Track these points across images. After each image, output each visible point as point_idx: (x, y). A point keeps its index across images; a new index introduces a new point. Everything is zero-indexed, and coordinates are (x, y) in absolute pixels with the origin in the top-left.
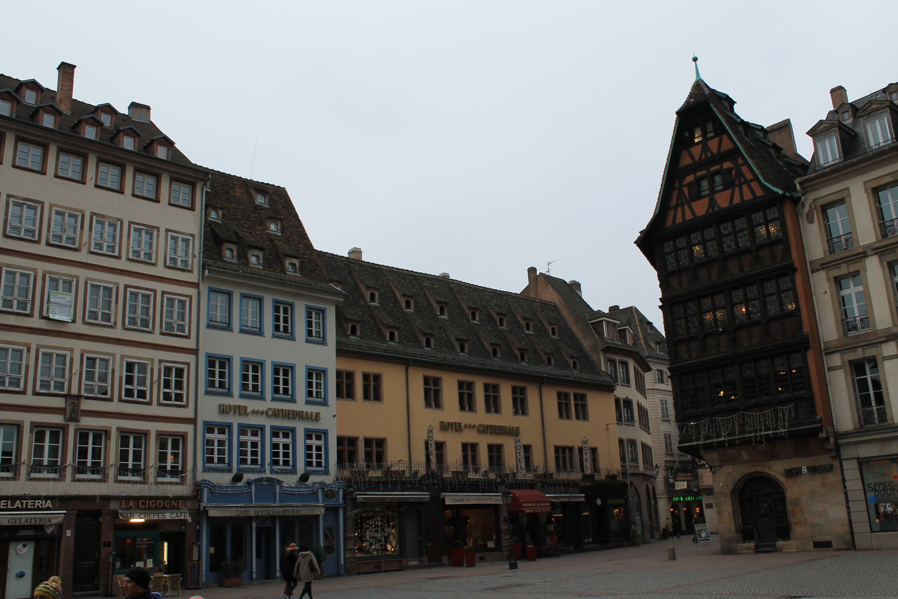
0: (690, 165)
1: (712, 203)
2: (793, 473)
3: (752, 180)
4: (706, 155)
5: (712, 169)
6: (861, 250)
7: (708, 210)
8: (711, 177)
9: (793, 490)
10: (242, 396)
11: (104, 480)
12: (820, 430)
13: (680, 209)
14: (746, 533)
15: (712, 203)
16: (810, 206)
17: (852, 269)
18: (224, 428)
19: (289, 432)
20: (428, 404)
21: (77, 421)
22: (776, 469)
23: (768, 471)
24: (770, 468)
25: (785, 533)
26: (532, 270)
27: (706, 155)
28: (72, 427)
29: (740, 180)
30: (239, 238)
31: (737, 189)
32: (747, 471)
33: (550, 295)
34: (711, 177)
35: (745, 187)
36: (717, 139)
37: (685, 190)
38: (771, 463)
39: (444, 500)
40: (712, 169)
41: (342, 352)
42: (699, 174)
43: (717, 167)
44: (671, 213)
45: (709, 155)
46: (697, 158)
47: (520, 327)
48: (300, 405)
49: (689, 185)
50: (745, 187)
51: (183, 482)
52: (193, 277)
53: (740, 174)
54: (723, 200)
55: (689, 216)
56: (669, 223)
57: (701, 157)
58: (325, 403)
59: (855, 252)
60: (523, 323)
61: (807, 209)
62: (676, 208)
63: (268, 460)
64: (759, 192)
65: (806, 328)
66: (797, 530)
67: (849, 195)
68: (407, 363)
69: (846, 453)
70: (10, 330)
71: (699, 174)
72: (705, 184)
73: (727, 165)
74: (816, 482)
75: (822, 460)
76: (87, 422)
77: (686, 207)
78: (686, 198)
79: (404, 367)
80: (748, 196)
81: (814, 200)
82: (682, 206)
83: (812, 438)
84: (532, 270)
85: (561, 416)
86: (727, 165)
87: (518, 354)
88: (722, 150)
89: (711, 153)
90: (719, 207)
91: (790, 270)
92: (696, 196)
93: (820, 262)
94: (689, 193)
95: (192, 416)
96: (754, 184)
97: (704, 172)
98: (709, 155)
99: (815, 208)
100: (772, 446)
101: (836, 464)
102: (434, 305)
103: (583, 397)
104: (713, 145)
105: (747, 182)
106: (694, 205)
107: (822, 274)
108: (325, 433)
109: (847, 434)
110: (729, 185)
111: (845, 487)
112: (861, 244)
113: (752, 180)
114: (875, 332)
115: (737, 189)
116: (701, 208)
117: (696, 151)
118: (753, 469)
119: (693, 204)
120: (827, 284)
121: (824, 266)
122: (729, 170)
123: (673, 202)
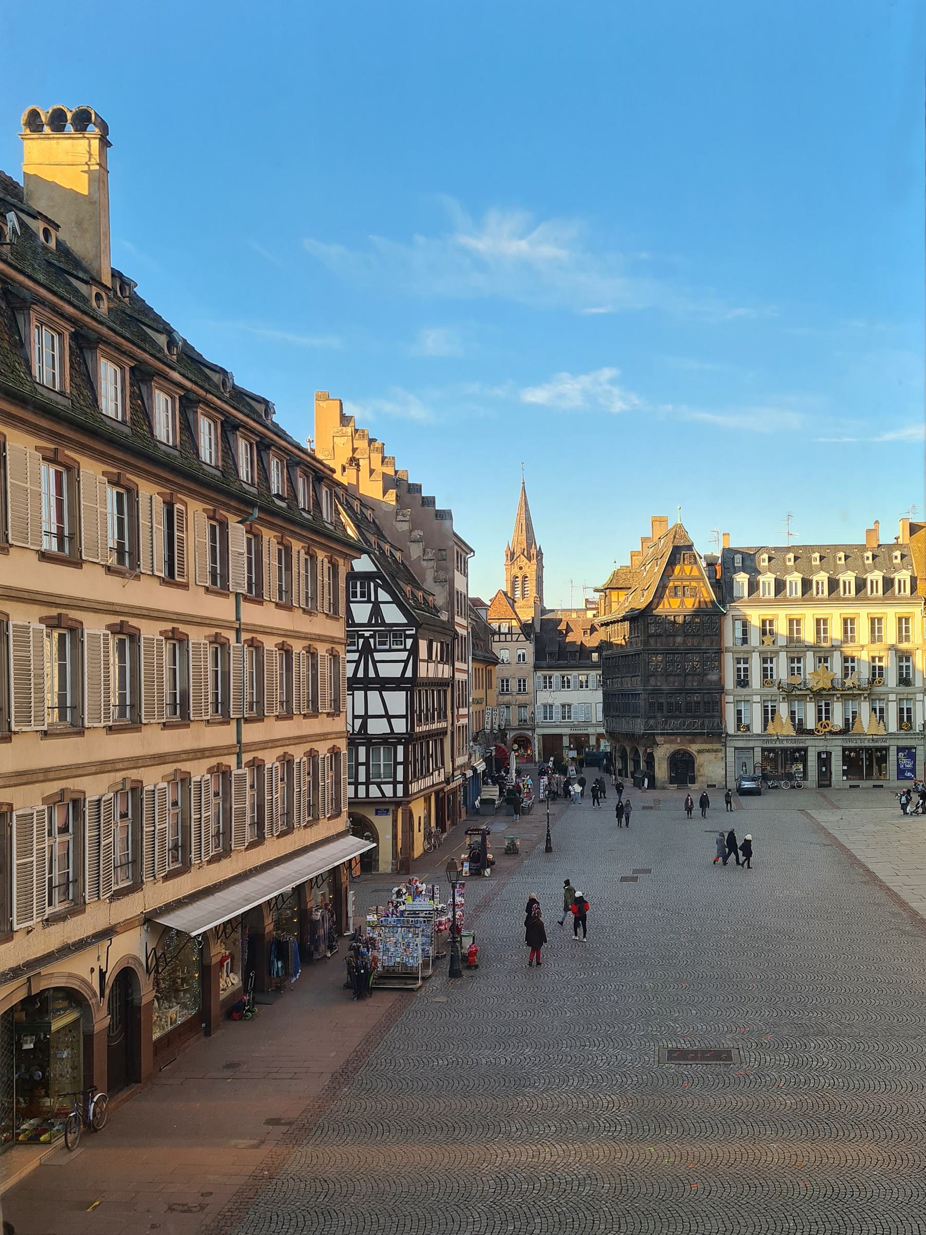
2: (699, 752)
9: (700, 759)
12: (722, 733)
14: (672, 780)
15: (682, 603)
22: (693, 748)
25: (693, 781)
66: (700, 779)
69: (728, 744)
73: (694, 584)
74: (712, 756)
75: (717, 746)
83: (717, 735)
86: (694, 584)
91: (720, 652)
100: (694, 737)
101: (723, 748)
109: (730, 736)
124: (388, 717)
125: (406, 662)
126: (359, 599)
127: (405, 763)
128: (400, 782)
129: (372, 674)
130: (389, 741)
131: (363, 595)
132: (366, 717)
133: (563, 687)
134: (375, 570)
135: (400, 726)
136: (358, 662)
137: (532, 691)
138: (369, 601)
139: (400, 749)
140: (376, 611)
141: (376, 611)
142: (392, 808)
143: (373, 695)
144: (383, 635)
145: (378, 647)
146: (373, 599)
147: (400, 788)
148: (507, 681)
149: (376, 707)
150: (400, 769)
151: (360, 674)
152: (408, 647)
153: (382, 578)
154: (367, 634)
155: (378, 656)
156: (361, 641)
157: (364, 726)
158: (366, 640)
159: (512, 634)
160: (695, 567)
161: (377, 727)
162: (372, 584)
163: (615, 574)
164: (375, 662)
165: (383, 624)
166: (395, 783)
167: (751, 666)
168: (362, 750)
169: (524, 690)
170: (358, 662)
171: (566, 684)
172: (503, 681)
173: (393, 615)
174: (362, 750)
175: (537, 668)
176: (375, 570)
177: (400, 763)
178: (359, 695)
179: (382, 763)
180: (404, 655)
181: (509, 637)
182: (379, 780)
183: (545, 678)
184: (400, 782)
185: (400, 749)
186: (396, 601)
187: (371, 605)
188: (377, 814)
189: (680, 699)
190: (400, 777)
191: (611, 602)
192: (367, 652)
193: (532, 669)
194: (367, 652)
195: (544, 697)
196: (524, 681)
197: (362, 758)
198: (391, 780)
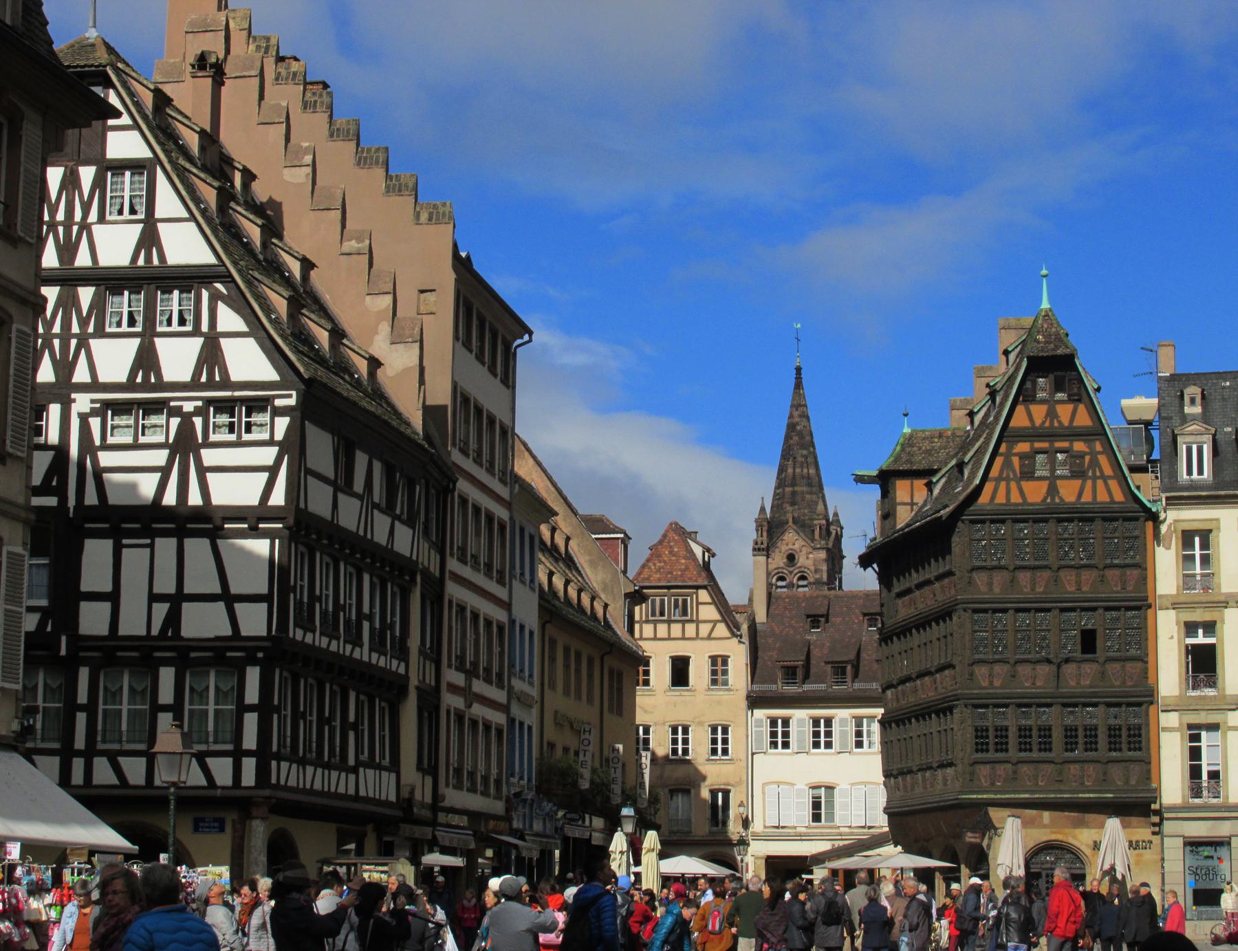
0: (1027, 428)
1: (1053, 490)
3: (1110, 477)
4: (1052, 422)
5: (1058, 445)
6: (1223, 598)
7: (1045, 499)
8: (1051, 453)
13: (1003, 484)
15: (1053, 490)
16: (1169, 527)
17: (1206, 616)
21: (470, 706)
23: (1071, 841)
24: (1075, 837)
27: (1052, 422)
29: (1094, 472)
31: (1089, 483)
32: (1045, 838)
34: (1051, 453)
35: (1100, 483)
36: (1070, 407)
37: (1015, 460)
38: (1077, 831)
40: (1058, 445)
42: (1038, 445)
43: (1065, 444)
44: (988, 488)
45: (1056, 424)
46: (1038, 422)
49: (1022, 456)
50: (1100, 483)
51: (498, 797)
52: (504, 492)
53: (1095, 463)
54: (1068, 492)
55: (1015, 498)
56: (984, 498)
57: (1044, 422)
59: (1216, 599)
61: (1164, 529)
62: (999, 479)
64: (1119, 496)
65: (1150, 681)
67: (1219, 528)
69: (1168, 827)
71: (1038, 445)
72: (1040, 458)
73: (1079, 446)
76: (478, 710)
77: (1013, 485)
78: (1014, 472)
80: (1102, 497)
81: (1175, 521)
82: (1008, 480)
83: (1139, 807)
88: (1075, 424)
89: (1060, 422)
90: (1061, 498)
91: (1139, 605)
92: (1028, 474)
93: (1172, 600)
94: (1021, 466)
96: (1113, 484)
97: (1045, 445)
98: (1056, 424)
99: (1175, 531)
101: (1156, 839)
103: (620, 675)
104: (1064, 412)
105: (1104, 478)
106: (1026, 485)
107: (1172, 613)
109: (1173, 808)
110: (1078, 473)
111: (1163, 867)
112: (1224, 590)
113: (1110, 477)
114: (1225, 696)
115: (1089, 483)
116: (1035, 492)
117: (1039, 412)
118: (1053, 837)
119: (1024, 484)
120: (1176, 628)
121: (1175, 606)
122: (1081, 456)
123: (994, 472)
124: (228, 598)
125: (273, 471)
126: (175, 327)
127: (265, 709)
128: (249, 753)
129: (195, 499)
130: (226, 654)
131: (182, 322)
132: (177, 599)
133: (816, 745)
134: (212, 260)
135: (254, 620)
136: (165, 471)
137: (743, 757)
138: (196, 332)
139: (253, 675)
140: (211, 355)
141: (211, 355)
142: (230, 817)
143: (197, 548)
144: (224, 406)
145: (213, 438)
146: (205, 327)
147: (249, 764)
148: (686, 731)
149: (201, 578)
150: (251, 721)
151: (170, 499)
152: (279, 435)
153: (227, 278)
155: (210, 457)
156: (175, 422)
157: (173, 619)
158: (187, 419)
159: (698, 622)
160: (1081, 407)
161: (202, 622)
162: (205, 295)
163: (910, 441)
164: (202, 471)
165: (226, 383)
166: (238, 755)
167: (1221, 641)
168: (167, 676)
169: (725, 752)
170: (165, 471)
171: (821, 737)
172: (675, 731)
173: (248, 362)
174: (167, 676)
175: (755, 701)
176: (212, 260)
177: (251, 708)
178: (166, 547)
179: (211, 707)
181: (690, 629)
182: (203, 747)
183: (773, 722)
184: (249, 753)
185: (253, 675)
186: (256, 330)
187: (198, 342)
188: (196, 829)
189: (1052, 717)
190: (250, 740)
191: (894, 505)
192: (185, 446)
193: (744, 704)
194: (185, 446)
195: (772, 766)
196: (725, 730)
197: (166, 695)
198: (229, 747)
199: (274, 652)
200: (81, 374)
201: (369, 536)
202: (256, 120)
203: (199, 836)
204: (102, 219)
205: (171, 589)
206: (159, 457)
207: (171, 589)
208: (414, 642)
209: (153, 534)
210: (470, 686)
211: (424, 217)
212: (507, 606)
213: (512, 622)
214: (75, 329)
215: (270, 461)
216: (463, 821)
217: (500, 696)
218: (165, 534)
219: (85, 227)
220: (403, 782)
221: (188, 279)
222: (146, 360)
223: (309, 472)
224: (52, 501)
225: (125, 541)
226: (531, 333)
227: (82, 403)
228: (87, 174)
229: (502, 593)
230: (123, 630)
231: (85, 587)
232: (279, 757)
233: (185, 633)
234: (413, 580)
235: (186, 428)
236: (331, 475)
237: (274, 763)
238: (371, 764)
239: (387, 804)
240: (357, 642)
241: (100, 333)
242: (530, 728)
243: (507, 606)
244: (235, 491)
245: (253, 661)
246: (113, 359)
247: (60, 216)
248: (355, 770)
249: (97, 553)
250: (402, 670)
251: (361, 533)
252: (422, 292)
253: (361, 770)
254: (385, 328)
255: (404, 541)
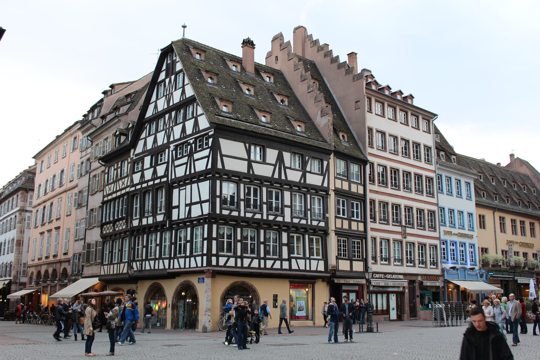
10: (450, 227)
11: (414, 266)
18: (444, 242)
19: (463, 245)
20: (501, 232)
21: (405, 238)
26: (512, 156)
28: (404, 241)
30: (442, 148)
33: (523, 170)
39: (517, 280)
41: (478, 205)
47: (521, 189)
48: (466, 232)
51: (437, 268)
52: (432, 168)
58: (473, 231)
60: (522, 187)
63: (459, 259)
68: (494, 209)
70: (383, 195)
76: (410, 239)
79: (491, 212)
84: (512, 156)
85: (531, 236)
87: (527, 204)
95: (438, 236)
102: (489, 177)
108: (474, 245)
125: (208, 157)
127: (210, 239)
129: (193, 171)
140: (196, 124)
141: (196, 124)
147: (205, 258)
151: (188, 173)
152: (210, 145)
154: (191, 141)
155: (196, 156)
156: (189, 147)
161: (196, 212)
165: (200, 131)
168: (189, 229)
170: (186, 163)
178: (188, 187)
180: (206, 152)
185: (206, 226)
187: (194, 119)
192: (191, 155)
199: (211, 219)
200: (172, 139)
201: (283, 177)
202: (287, 60)
203: (199, 284)
204: (176, 89)
205: (189, 202)
206: (185, 160)
207: (189, 202)
208: (331, 214)
209: (185, 184)
210: (405, 231)
211: (356, 79)
212: (437, 205)
213: (442, 209)
214: (171, 125)
215: (208, 154)
216: (401, 277)
217: (436, 235)
218: (188, 184)
219: (172, 94)
220: (329, 263)
221: (192, 101)
222: (184, 130)
223: (222, 156)
224: (164, 179)
225: (181, 188)
226: (437, 115)
227: (172, 147)
228: (173, 77)
229: (434, 201)
230: (180, 218)
231: (173, 205)
232: (217, 256)
233: (192, 216)
234: (328, 194)
235: (191, 148)
236: (247, 158)
237: (214, 259)
238: (304, 258)
239: (317, 271)
240: (283, 215)
241: (176, 124)
242: (472, 246)
243: (437, 205)
244: (201, 166)
245: (205, 223)
246: (177, 130)
247: (168, 93)
248: (289, 260)
249: (176, 192)
250: (322, 224)
251: (276, 176)
252: (356, 102)
253: (293, 261)
254: (319, 112)
255: (314, 180)
